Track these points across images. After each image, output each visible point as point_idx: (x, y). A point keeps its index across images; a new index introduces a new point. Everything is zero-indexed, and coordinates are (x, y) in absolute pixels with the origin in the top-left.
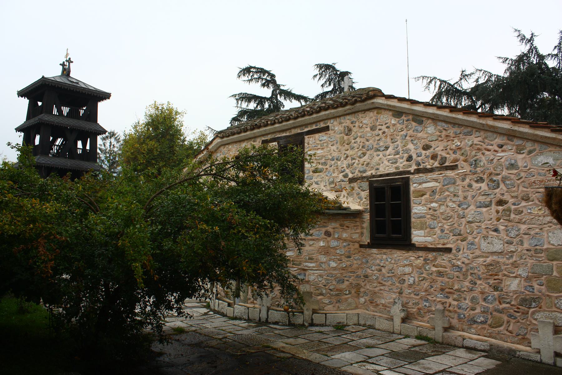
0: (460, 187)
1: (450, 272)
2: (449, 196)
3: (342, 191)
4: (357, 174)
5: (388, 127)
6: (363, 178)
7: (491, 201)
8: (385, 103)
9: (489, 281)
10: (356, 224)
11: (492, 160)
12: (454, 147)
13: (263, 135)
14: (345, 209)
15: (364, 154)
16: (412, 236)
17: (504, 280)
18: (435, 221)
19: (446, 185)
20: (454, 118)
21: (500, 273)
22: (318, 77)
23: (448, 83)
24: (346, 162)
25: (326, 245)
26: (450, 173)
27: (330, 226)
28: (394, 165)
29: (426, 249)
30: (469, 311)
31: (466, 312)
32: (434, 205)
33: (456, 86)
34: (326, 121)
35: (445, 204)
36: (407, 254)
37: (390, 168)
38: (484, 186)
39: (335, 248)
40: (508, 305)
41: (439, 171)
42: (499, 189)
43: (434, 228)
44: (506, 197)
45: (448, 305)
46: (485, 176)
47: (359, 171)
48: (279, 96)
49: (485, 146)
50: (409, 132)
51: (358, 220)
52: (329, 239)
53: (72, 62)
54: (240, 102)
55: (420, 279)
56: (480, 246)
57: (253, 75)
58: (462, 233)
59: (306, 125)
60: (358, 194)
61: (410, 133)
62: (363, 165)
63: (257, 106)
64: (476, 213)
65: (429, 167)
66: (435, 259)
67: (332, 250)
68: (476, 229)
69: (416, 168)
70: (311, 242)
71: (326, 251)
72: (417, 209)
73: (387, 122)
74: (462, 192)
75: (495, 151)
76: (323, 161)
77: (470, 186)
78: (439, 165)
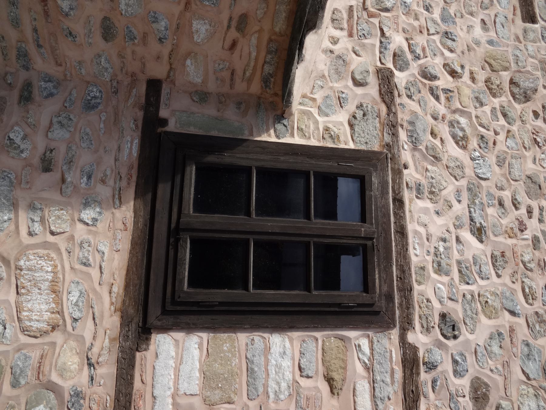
3: (351, 35)
6: (393, 127)
10: (238, 80)
15: (461, 142)
16: (179, 335)
24: (436, 64)
47: (414, 113)
50: (521, 321)
51: (256, 88)
60: (341, 102)
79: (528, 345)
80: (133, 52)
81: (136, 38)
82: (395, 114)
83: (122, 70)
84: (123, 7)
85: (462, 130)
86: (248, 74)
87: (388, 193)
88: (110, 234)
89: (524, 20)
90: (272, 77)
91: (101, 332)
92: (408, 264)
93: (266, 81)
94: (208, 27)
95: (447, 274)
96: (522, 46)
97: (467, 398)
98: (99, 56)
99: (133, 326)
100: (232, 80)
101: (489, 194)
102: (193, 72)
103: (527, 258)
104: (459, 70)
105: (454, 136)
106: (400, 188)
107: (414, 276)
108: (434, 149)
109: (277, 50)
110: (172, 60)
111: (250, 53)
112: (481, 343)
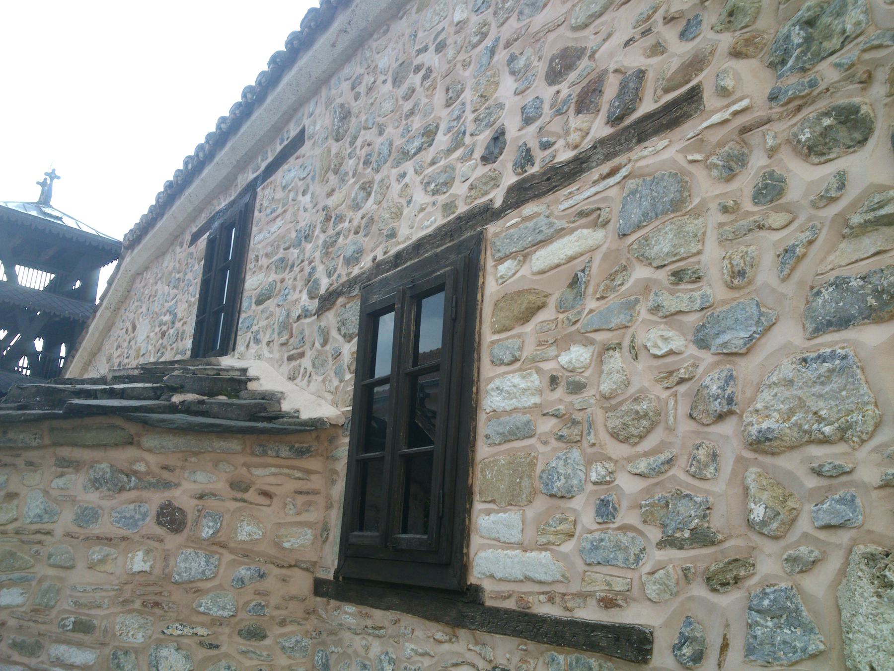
2: (647, 287)
3: (302, 355)
4: (343, 273)
10: (308, 486)
14: (278, 416)
15: (366, 189)
18: (576, 454)
19: (639, 227)
25: (157, 571)
26: (661, 153)
27: (186, 485)
28: (441, 199)
29: (525, 625)
32: (577, 355)
35: (626, 343)
37: (430, 214)
39: (192, 587)
41: (608, 157)
43: (565, 496)
51: (313, 464)
52: (173, 541)
53: (58, 178)
56: (843, 632)
58: (716, 522)
60: (337, 355)
62: (357, 233)
65: (565, 156)
67: (178, 596)
70: (97, 553)
71: (151, 597)
74: (723, 241)
77: (770, 190)
78: (608, 131)
80: (277, 608)
81: (260, 604)
82: (343, 285)
83: (302, 625)
84: (226, 613)
86: (299, 474)
87: (387, 277)
88: (401, 640)
90: (294, 446)
91: (470, 657)
92: (439, 229)
93: (301, 453)
94: (245, 523)
98: (283, 648)
100: (308, 493)
102: (299, 540)
106: (387, 262)
107: (452, 217)
109: (260, 445)
110: (285, 564)
111: (274, 474)
112: (515, 85)
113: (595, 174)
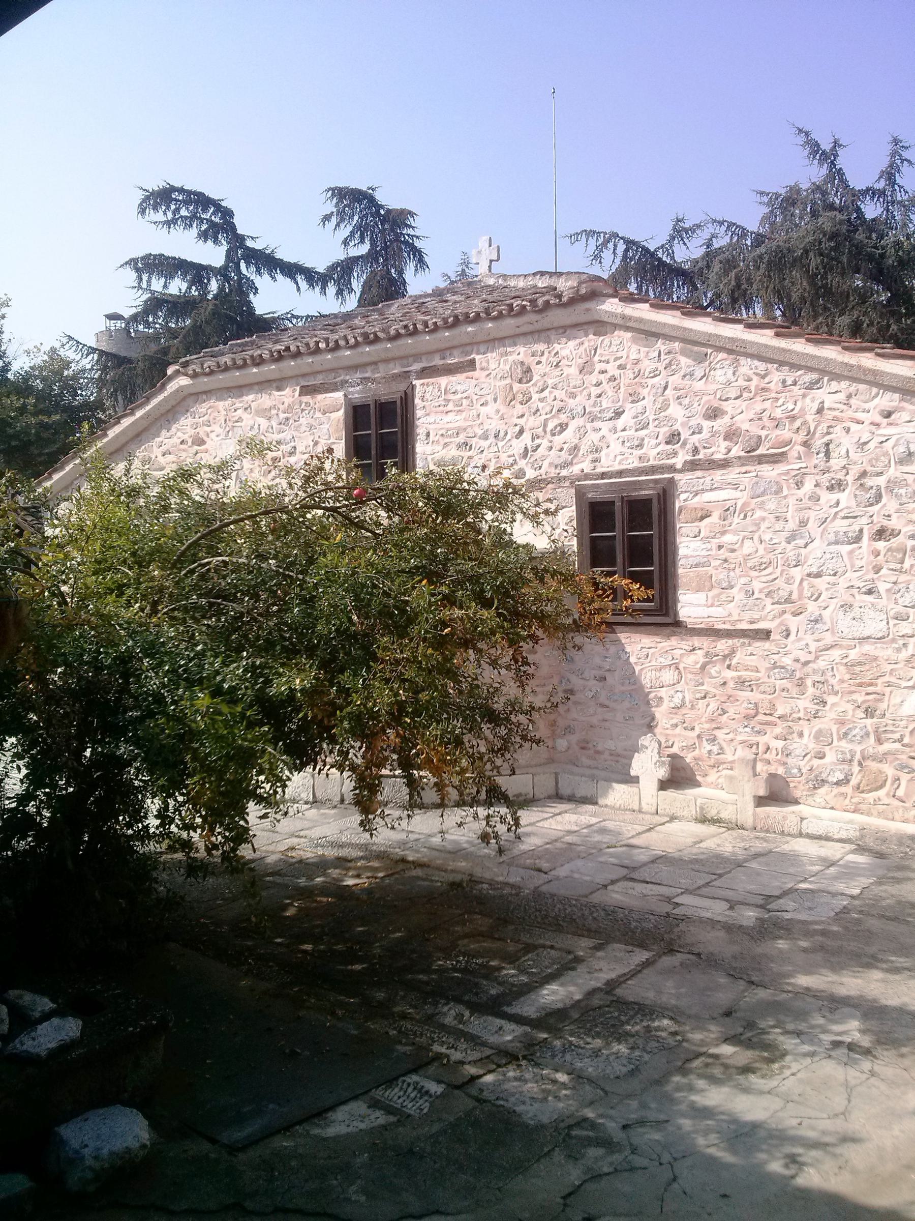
0: (792, 501)
1: (766, 680)
2: (763, 519)
4: (547, 470)
5: (621, 367)
6: (560, 479)
7: (861, 531)
8: (619, 311)
9: (855, 697)
11: (866, 443)
12: (778, 413)
13: (304, 376)
15: (563, 427)
16: (679, 605)
17: (887, 694)
20: (784, 350)
21: (880, 681)
22: (334, 220)
23: (643, 248)
26: (769, 472)
30: (810, 760)
31: (802, 763)
33: (660, 254)
34: (468, 348)
35: (756, 538)
36: (666, 644)
38: (845, 498)
40: (897, 745)
41: (743, 465)
42: (880, 505)
44: (894, 523)
45: (762, 748)
46: (850, 479)
47: (551, 464)
48: (243, 265)
49: (850, 413)
50: (671, 379)
54: (145, 277)
55: (698, 696)
56: (834, 623)
57: (177, 210)
59: (417, 357)
61: (675, 380)
62: (561, 450)
63: (189, 288)
64: (828, 556)
65: (719, 456)
66: (733, 652)
68: (827, 589)
69: (689, 458)
72: (689, 547)
73: (619, 354)
75: (872, 424)
76: (461, 438)
78: (743, 454)
79: (684, 376)
85: (556, 427)
89: (475, 370)
92: (638, 468)
95: (643, 440)
96: (494, 373)
97: (714, 424)
99: (675, 629)
101: (594, 405)
103: (632, 376)
104: (518, 428)
105: (561, 432)
108: (570, 450)
112: (684, 412)
113: (738, 470)
